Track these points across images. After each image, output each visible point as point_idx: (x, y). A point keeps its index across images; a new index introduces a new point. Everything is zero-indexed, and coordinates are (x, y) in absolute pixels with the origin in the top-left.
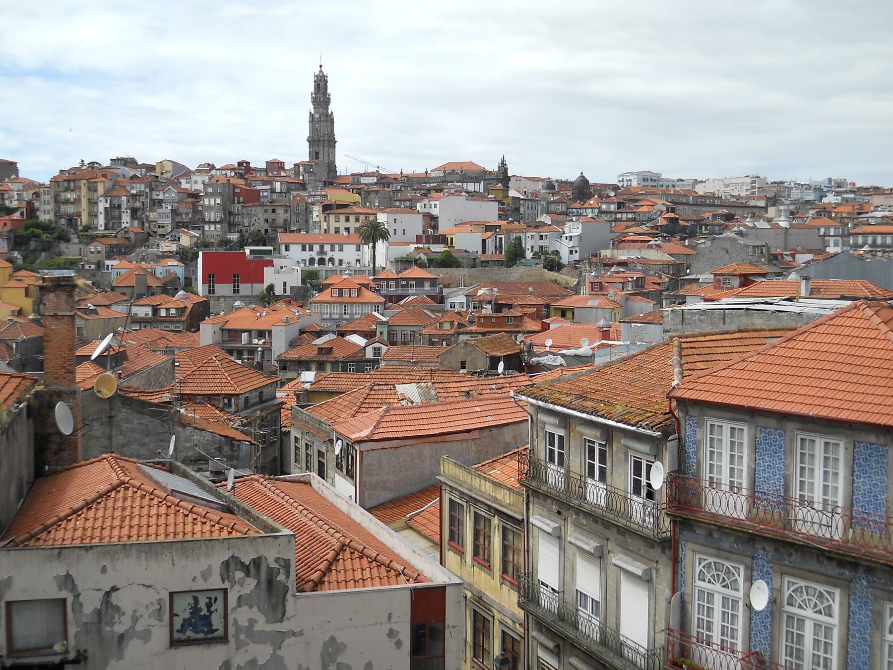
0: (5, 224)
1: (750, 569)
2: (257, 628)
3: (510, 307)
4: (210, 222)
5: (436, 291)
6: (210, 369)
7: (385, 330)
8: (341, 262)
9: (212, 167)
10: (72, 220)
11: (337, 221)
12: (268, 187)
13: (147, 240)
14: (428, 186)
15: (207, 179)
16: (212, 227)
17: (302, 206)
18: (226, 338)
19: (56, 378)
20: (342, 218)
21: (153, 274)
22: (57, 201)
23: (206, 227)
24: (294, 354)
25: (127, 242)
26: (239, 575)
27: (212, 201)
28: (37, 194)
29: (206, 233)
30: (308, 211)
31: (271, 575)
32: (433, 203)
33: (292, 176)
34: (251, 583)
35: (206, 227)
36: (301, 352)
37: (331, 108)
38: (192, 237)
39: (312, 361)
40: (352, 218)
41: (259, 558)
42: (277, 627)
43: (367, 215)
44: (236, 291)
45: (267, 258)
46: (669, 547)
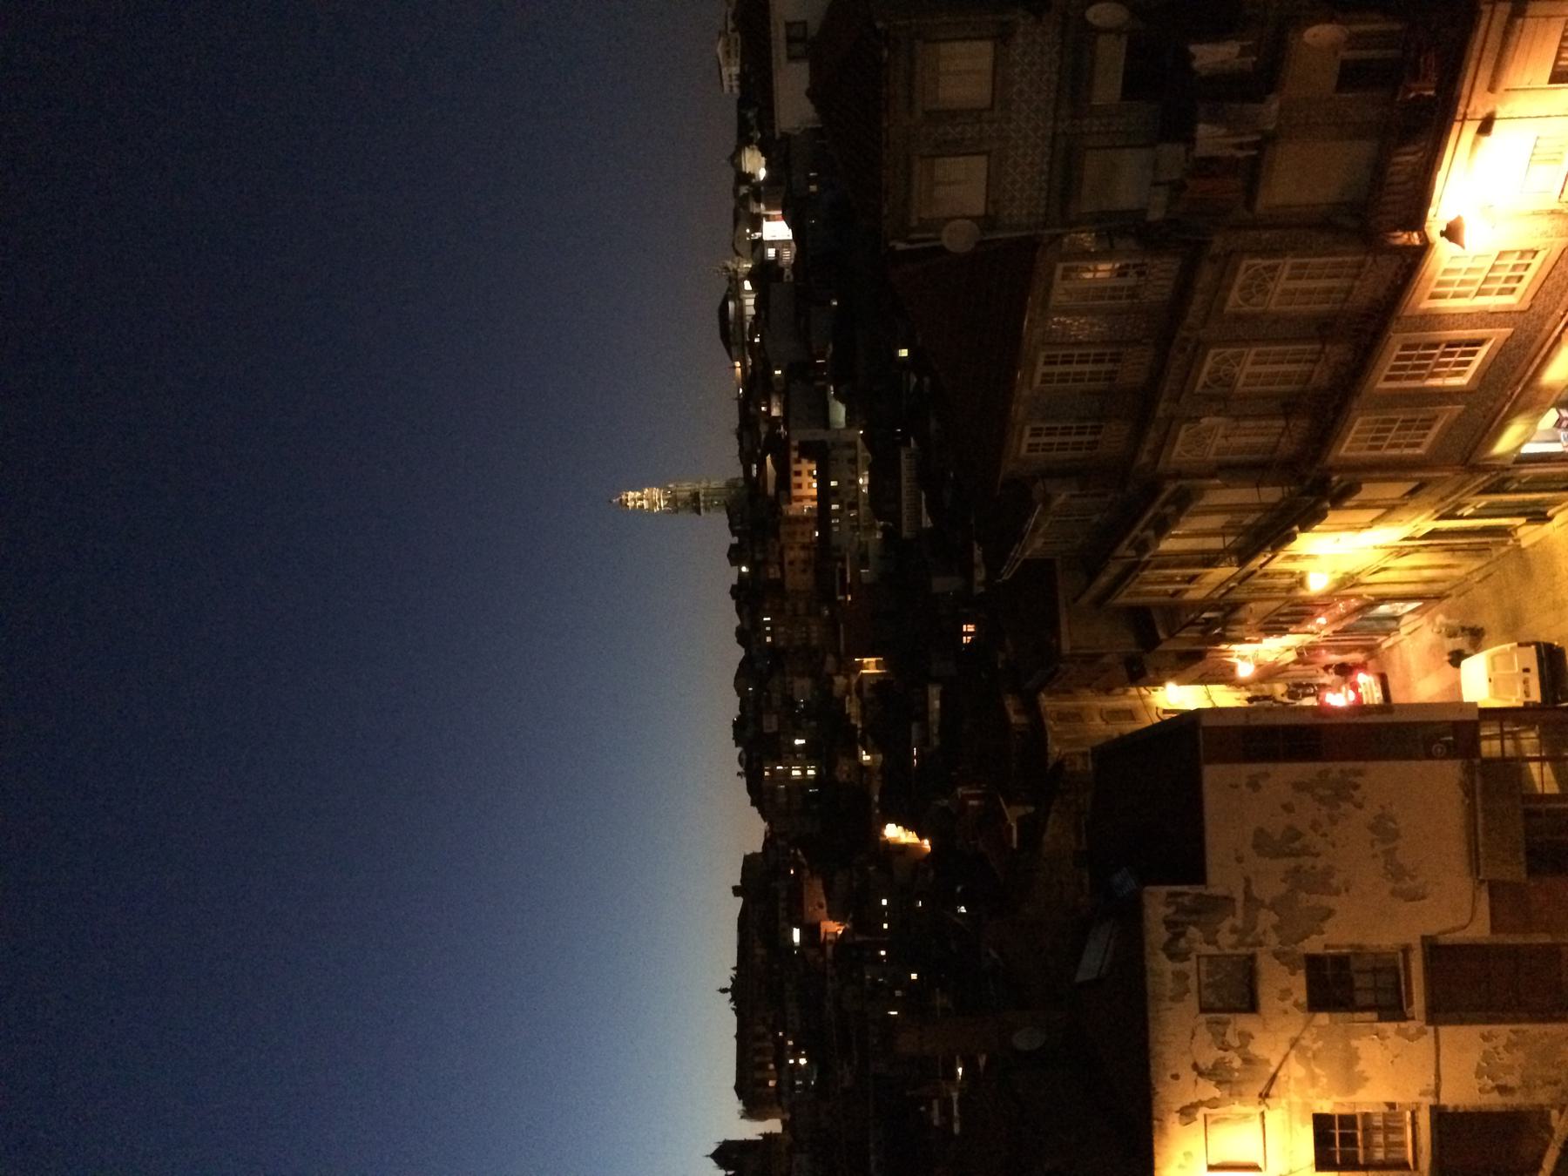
1: (1189, 419)
2: (1239, 923)
16: (815, 635)
23: (815, 642)
26: (1182, 943)
31: (1181, 909)
34: (1193, 931)
41: (1165, 922)
42: (1239, 904)
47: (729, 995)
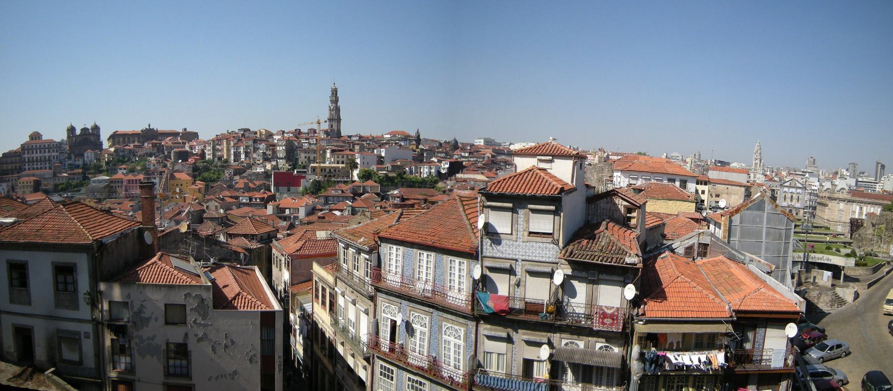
3: (408, 199)
4: (280, 158)
9: (283, 132)
10: (220, 158)
30: (325, 152)
43: (353, 155)
44: (289, 190)
46: (372, 298)
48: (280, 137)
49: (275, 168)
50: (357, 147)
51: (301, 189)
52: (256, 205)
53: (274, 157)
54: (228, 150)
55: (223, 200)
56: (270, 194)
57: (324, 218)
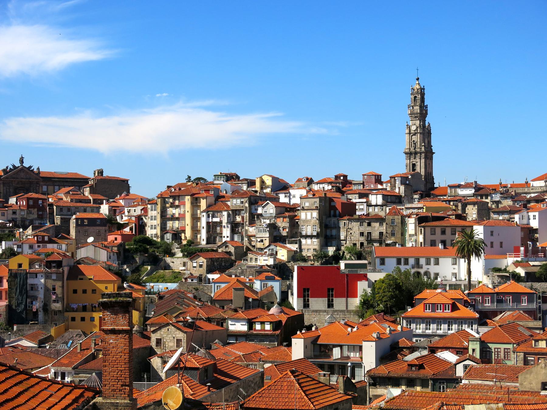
0: (116, 239)
4: (306, 237)
5: (534, 306)
6: (285, 384)
7: (477, 346)
8: (437, 275)
9: (310, 182)
11: (433, 233)
12: (364, 200)
13: (246, 254)
14: (528, 196)
15: (304, 192)
16: (309, 241)
17: (398, 219)
18: (317, 353)
19: (114, 390)
20: (438, 231)
21: (251, 288)
22: (164, 217)
23: (303, 241)
24: (384, 370)
25: (227, 256)
27: (309, 214)
28: (145, 210)
29: (303, 247)
30: (403, 224)
32: (531, 214)
33: (389, 189)
35: (303, 241)
36: (391, 369)
37: (428, 120)
38: (289, 251)
39: (402, 378)
40: (448, 231)
43: (463, 229)
44: (330, 305)
45: (361, 272)
47: (18, 164)
48: (304, 192)
49: (296, 257)
50: (472, 212)
51: (356, 302)
52: (262, 337)
53: (295, 233)
54: (195, 219)
55: (191, 325)
56: (293, 314)
57: (421, 367)
